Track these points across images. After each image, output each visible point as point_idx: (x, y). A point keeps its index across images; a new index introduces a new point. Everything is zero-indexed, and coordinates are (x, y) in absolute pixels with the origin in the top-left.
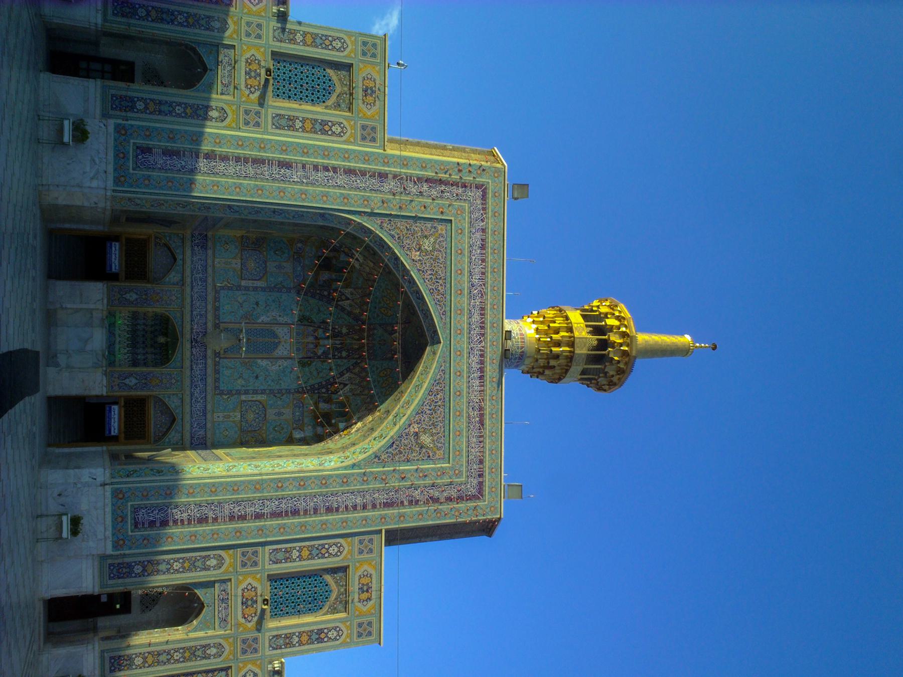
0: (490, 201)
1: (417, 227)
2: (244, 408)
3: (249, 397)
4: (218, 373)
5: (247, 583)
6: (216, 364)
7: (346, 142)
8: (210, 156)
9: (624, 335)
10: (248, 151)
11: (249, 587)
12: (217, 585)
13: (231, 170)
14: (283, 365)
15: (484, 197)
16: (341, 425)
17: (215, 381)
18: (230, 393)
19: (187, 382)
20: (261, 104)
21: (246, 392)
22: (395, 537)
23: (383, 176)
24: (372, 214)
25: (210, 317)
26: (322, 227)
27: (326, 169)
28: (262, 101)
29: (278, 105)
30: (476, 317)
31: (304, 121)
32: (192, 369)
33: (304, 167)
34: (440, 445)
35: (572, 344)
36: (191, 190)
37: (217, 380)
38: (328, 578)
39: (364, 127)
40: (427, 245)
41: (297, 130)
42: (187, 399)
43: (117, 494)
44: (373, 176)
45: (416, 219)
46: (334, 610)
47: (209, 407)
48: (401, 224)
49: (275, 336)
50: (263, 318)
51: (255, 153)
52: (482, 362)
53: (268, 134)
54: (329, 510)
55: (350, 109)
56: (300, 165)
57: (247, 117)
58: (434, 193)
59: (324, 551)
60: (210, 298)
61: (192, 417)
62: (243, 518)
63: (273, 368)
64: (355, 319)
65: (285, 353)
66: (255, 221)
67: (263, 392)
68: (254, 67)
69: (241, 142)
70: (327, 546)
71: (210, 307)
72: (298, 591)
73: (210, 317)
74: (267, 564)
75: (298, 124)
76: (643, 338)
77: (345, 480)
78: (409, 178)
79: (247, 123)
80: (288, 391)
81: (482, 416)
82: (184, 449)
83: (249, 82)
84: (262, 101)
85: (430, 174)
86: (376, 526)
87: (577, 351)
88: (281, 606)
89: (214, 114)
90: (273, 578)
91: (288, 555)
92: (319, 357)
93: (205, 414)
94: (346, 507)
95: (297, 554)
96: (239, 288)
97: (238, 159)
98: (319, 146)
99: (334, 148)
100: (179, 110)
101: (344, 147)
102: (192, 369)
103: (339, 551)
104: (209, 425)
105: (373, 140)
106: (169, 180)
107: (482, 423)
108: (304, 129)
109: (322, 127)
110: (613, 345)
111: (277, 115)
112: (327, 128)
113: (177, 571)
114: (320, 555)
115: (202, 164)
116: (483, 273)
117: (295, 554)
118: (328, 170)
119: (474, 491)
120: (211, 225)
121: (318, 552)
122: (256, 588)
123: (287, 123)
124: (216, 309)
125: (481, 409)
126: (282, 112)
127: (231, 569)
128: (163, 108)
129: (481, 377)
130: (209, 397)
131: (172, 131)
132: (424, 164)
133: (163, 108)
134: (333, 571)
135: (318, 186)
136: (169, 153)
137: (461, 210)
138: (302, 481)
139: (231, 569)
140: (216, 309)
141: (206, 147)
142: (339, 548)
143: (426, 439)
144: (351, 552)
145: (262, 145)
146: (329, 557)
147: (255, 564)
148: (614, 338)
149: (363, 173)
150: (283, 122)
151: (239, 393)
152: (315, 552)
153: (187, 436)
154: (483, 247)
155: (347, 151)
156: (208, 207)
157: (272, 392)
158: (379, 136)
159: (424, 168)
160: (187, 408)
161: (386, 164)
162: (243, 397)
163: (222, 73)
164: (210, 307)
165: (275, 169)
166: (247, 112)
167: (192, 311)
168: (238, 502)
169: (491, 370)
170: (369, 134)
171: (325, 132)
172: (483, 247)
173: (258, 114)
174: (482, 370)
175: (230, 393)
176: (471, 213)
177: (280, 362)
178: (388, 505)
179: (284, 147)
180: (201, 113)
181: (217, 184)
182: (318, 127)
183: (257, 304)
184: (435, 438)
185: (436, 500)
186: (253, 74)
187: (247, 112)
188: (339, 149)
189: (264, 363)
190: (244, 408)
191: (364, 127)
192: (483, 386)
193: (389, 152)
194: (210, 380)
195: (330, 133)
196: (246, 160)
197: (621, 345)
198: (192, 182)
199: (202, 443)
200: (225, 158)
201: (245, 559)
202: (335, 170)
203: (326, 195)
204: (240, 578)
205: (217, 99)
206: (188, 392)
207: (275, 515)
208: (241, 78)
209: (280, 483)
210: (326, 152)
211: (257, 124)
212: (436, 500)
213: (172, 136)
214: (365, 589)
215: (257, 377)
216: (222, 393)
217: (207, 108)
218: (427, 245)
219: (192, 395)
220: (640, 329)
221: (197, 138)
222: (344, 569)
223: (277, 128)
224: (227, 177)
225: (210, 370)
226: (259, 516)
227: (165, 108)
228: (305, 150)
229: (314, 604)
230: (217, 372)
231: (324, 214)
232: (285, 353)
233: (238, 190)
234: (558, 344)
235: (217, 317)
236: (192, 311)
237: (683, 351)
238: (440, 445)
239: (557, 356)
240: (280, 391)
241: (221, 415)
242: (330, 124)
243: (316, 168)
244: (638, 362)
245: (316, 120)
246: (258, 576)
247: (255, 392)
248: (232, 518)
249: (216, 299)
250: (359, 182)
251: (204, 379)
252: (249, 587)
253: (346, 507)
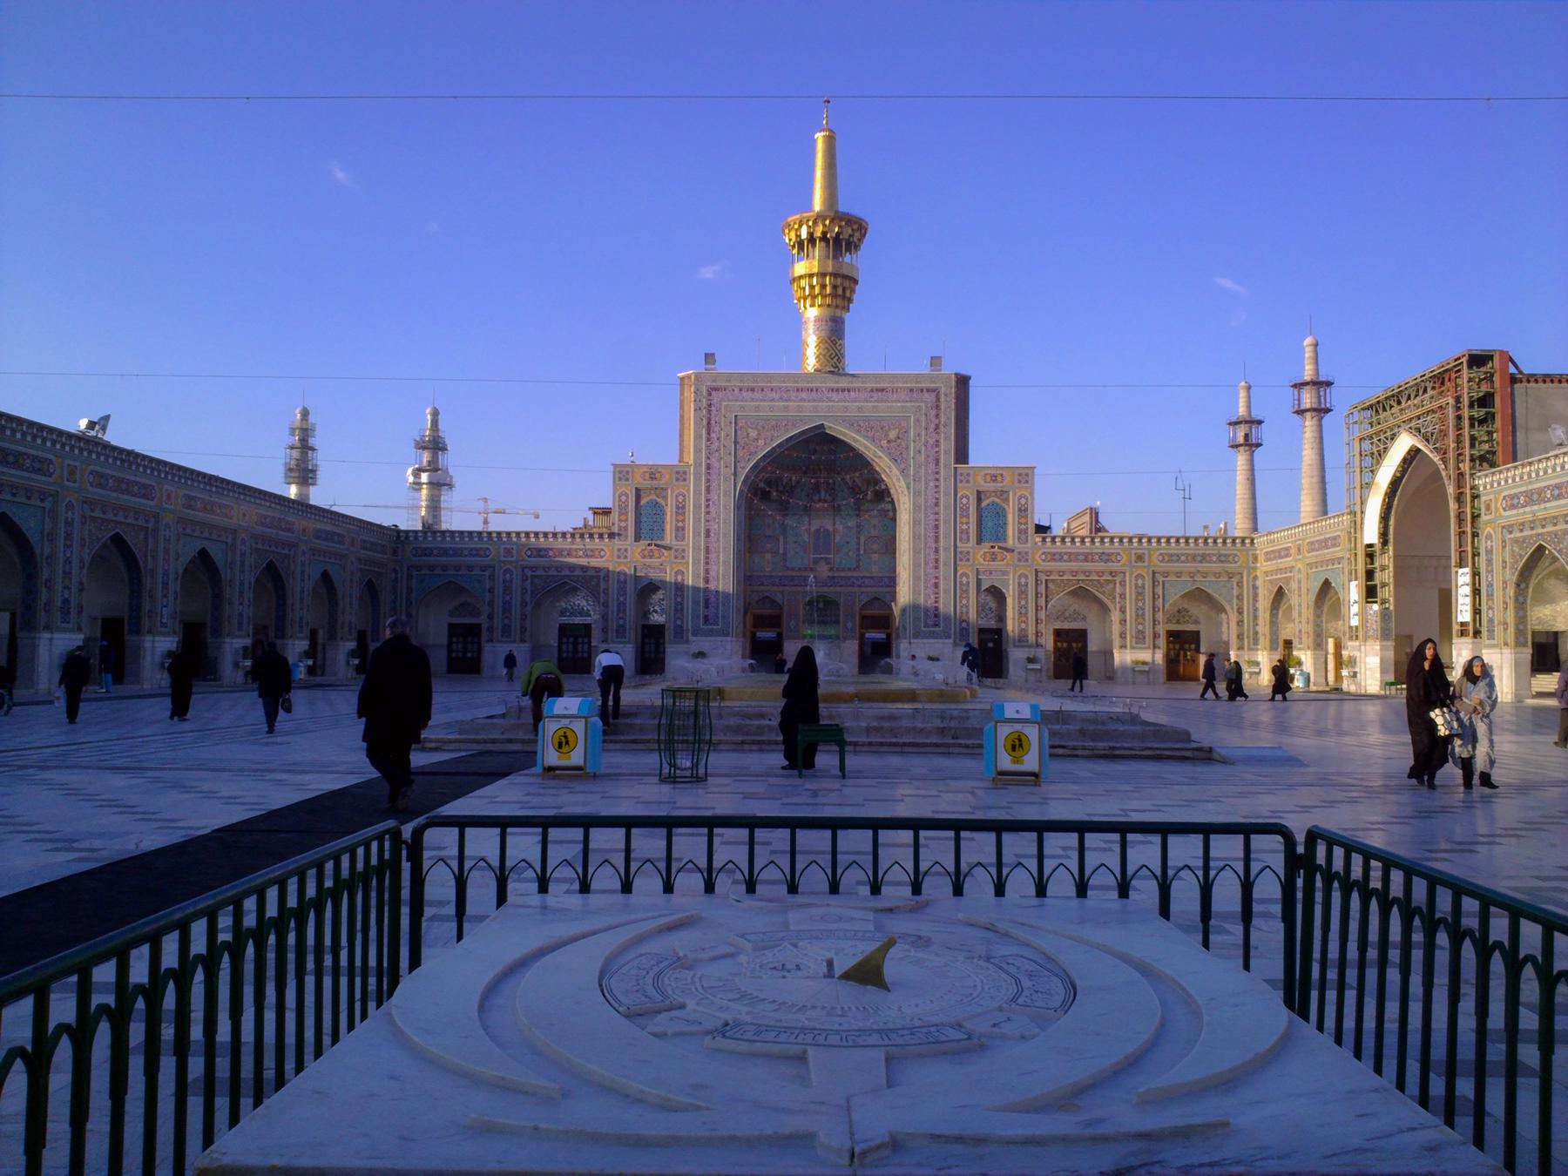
0: (718, 384)
1: (742, 442)
9: (815, 222)
10: (700, 554)
14: (841, 527)
15: (716, 389)
22: (962, 455)
23: (709, 467)
24: (735, 474)
29: (669, 537)
35: (822, 275)
38: (984, 504)
40: (753, 434)
43: (916, 636)
45: (736, 443)
46: (1007, 500)
48: (740, 453)
49: (818, 531)
54: (937, 504)
62: (937, 561)
72: (989, 523)
77: (917, 494)
81: (878, 390)
87: (830, 269)
88: (999, 535)
89: (680, 578)
107: (882, 390)
109: (681, 509)
110: (824, 233)
119: (933, 395)
120: (747, 578)
123: (680, 531)
132: (698, 437)
134: (979, 500)
138: (915, 523)
145: (696, 549)
179: (696, 533)
185: (937, 427)
189: (838, 538)
194: (850, 574)
200: (707, 572)
207: (937, 540)
208: (655, 561)
209: (916, 537)
210: (697, 506)
212: (937, 427)
214: (994, 478)
218: (753, 434)
222: (979, 493)
226: (937, 551)
228: (697, 520)
229: (1000, 514)
231: (738, 507)
234: (823, 286)
239: (835, 287)
244: (842, 208)
250: (714, 484)
251: (849, 578)
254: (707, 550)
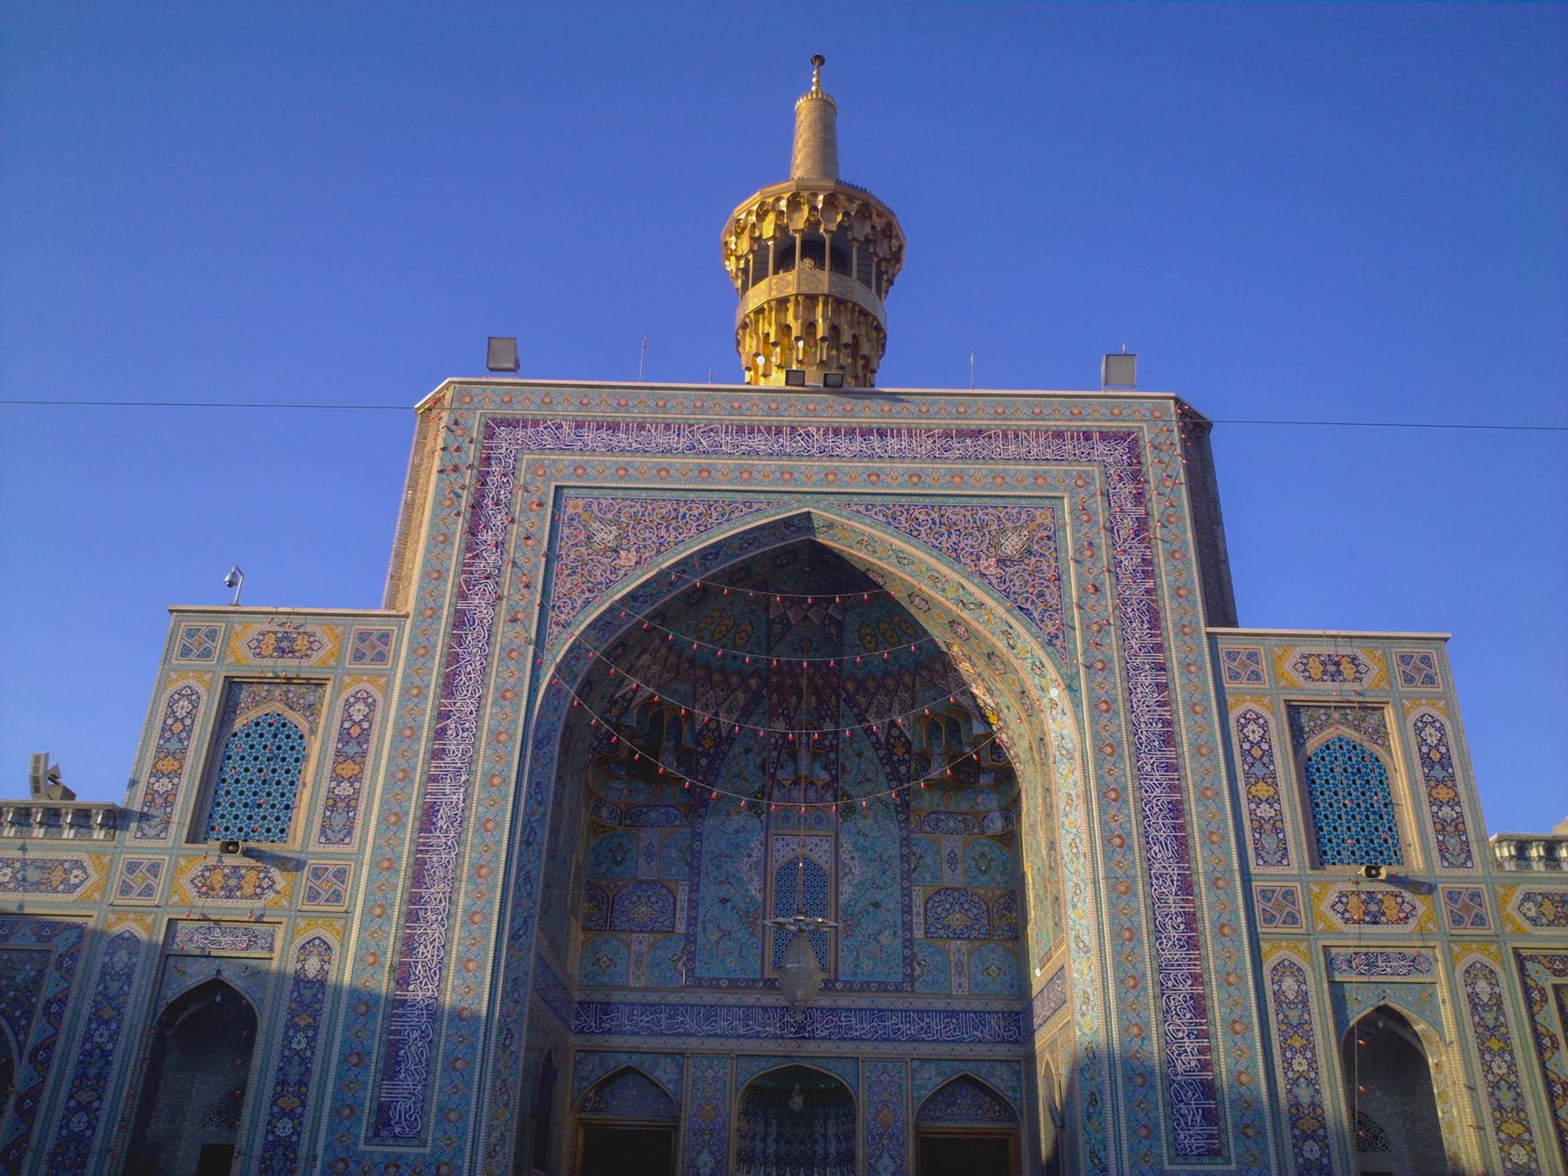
2: (942, 932)
3: (918, 921)
4: (868, 983)
5: (1330, 913)
6: (849, 988)
7: (387, 693)
8: (403, 976)
9: (794, 204)
10: (395, 893)
11: (1340, 907)
12: (1338, 978)
13: (436, 931)
14: (851, 850)
16: (978, 729)
17: (885, 990)
18: (909, 961)
19: (886, 1049)
20: (299, 865)
21: (908, 927)
23: (461, 620)
25: (750, 999)
26: (565, 749)
27: (441, 733)
28: (292, 865)
30: (758, 442)
31: (338, 778)
32: (860, 1039)
33: (433, 779)
34: (1024, 516)
36: (475, 1017)
37: (883, 988)
39: (359, 656)
41: (357, 792)
42: (925, 1050)
44: (460, 640)
45: (551, 556)
47: (939, 1005)
50: (754, 888)
51: (401, 881)
52: (851, 432)
53: (361, 852)
55: (320, 684)
56: (432, 787)
57: (324, 896)
58: (499, 520)
59: (1256, 752)
61: (961, 1041)
63: (856, 871)
64: (757, 692)
65: (826, 846)
66: (547, 886)
67: (907, 893)
68: (217, 879)
69: (376, 911)
70: (1246, 746)
73: (750, 999)
74: (1287, 871)
75: (345, 789)
76: (801, 164)
78: (466, 568)
79: (337, 897)
80: (906, 841)
82: (1030, 1059)
83: (249, 890)
84: (292, 865)
85: (460, 525)
86: (1199, 645)
89: (312, 967)
90: (1319, 859)
91: (1268, 827)
92: (835, 779)
94: (1161, 704)
95: (1264, 806)
97: (412, 917)
98: (393, 747)
99: (399, 717)
100: (300, 1042)
101: (398, 696)
102: (860, 1039)
103: (1255, 721)
104: (978, 1005)
105: (384, 638)
106: (450, 1066)
108: (355, 779)
109: (354, 741)
110: (813, 225)
111: (323, 833)
112: (355, 731)
113: (1312, 1063)
114: (1266, 760)
115: (418, 993)
116: (667, 427)
117: (1265, 811)
118: (444, 730)
121: (1258, 764)
122: (1342, 894)
124: (734, 985)
125: (947, 435)
126: (318, 822)
127: (1303, 947)
128: (293, 1077)
129: (882, 434)
130: (920, 1004)
131: (344, 1058)
132: (440, 539)
133: (293, 1077)
135: (477, 751)
136: (391, 1067)
137: (536, 469)
139: (1303, 947)
140: (734, 985)
141: (383, 984)
142: (1249, 721)
143: (1012, 544)
144: (1257, 697)
145: (384, 864)
146: (1269, 742)
147: (1289, 894)
148: (800, 221)
149: (453, 658)
150: (338, 820)
151: (909, 943)
152: (1259, 770)
153: (1002, 1051)
154: (613, 427)
155: (405, 691)
156: (514, 984)
157: (906, 875)
158: (377, 626)
159: (447, 540)
160: (943, 1050)
161: (435, 613)
162: (919, 933)
163: (228, 946)
165: (437, 838)
166: (313, 896)
167: (739, 1036)
169: (866, 413)
170: (373, 647)
171: (364, 736)
172: (613, 427)
173: (317, 873)
174: (866, 433)
175: (909, 961)
176: (542, 449)
177: (845, 857)
178: (1154, 619)
179: (392, 818)
180: (309, 993)
181: (463, 963)
182: (352, 749)
183: (724, 901)
184: (1009, 524)
186: (233, 882)
187: (313, 896)
188: (400, 706)
189: (847, 890)
190: (942, 932)
191: (359, 656)
192: (899, 431)
193: (410, 608)
194: (883, 1002)
195: (365, 725)
196: (415, 899)
197: (813, 208)
198: (457, 1016)
199: (1018, 1022)
200: (409, 945)
201: (1280, 917)
202: (443, 716)
203: (495, 736)
204: (1321, 926)
205: (282, 957)
206: (909, 1047)
208: (241, 907)
210: (408, 733)
211: (341, 874)
213: (354, 1057)
215: (876, 905)
216: (911, 978)
217: (299, 980)
219: (913, 1039)
220: (786, 176)
221: (362, 1001)
223: (349, 833)
224: (449, 940)
225: (863, 1002)
227: (294, 1074)
230: (865, 987)
232: (826, 846)
233: (477, 918)
234: (810, 326)
235: (750, 985)
236: (739, 1036)
237: (827, 112)
238: (1024, 516)
240: (905, 859)
241: (955, 980)
242: (347, 725)
243: (437, 754)
245: (338, 753)
246: (1316, 889)
247: (907, 909)
249: (714, 984)
251: (880, 1014)
252: (1340, 907)
253: (1161, 704)
254: (419, 875)
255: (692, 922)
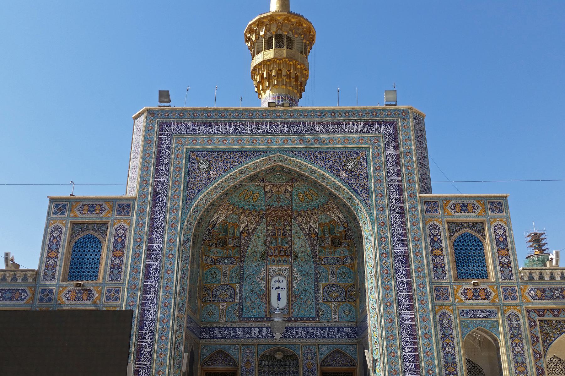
2: (329, 299)
3: (321, 296)
6: (296, 320)
7: (130, 225)
17: (309, 320)
21: (317, 298)
25: (262, 325)
27: (150, 240)
31: (114, 257)
32: (300, 338)
33: (149, 256)
37: (308, 319)
41: (122, 262)
42: (323, 341)
47: (328, 325)
53: (124, 283)
56: (148, 259)
60: (248, 325)
61: (336, 337)
62: (411, 299)
63: (298, 279)
65: (287, 270)
66: (190, 291)
67: (316, 286)
71: (255, 325)
73: (262, 325)
75: (117, 261)
80: (316, 268)
93: (333, 328)
96: (240, 304)
98: (134, 246)
102: (300, 338)
104: (341, 325)
109: (120, 243)
112: (120, 240)
118: (152, 239)
123: (116, 269)
124: (256, 320)
130: (320, 325)
135: (163, 246)
140: (256, 320)
151: (317, 303)
155: (137, 225)
162: (321, 300)
164: (255, 325)
167: (258, 338)
168: (399, 303)
171: (123, 242)
175: (317, 310)
177: (295, 274)
179: (135, 271)
183: (252, 291)
190: (329, 299)
194: (308, 325)
195: (123, 238)
196: (144, 299)
202: (151, 234)
206: (318, 340)
207: (408, 275)
210: (138, 240)
215: (306, 291)
216: (318, 316)
219: (319, 337)
224: (157, 313)
225: (301, 325)
226: (409, 287)
230: (302, 319)
232: (287, 270)
235: (262, 320)
236: (258, 338)
241: (334, 316)
242: (116, 238)
243: (149, 247)
245: (114, 248)
247: (316, 292)
248: (411, 307)
249: (249, 320)
251: (308, 329)
255: (241, 298)
